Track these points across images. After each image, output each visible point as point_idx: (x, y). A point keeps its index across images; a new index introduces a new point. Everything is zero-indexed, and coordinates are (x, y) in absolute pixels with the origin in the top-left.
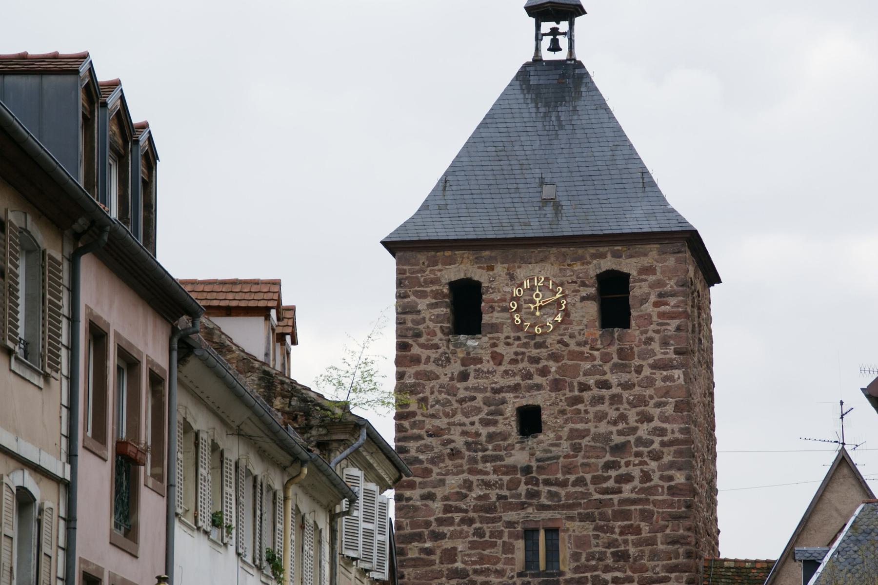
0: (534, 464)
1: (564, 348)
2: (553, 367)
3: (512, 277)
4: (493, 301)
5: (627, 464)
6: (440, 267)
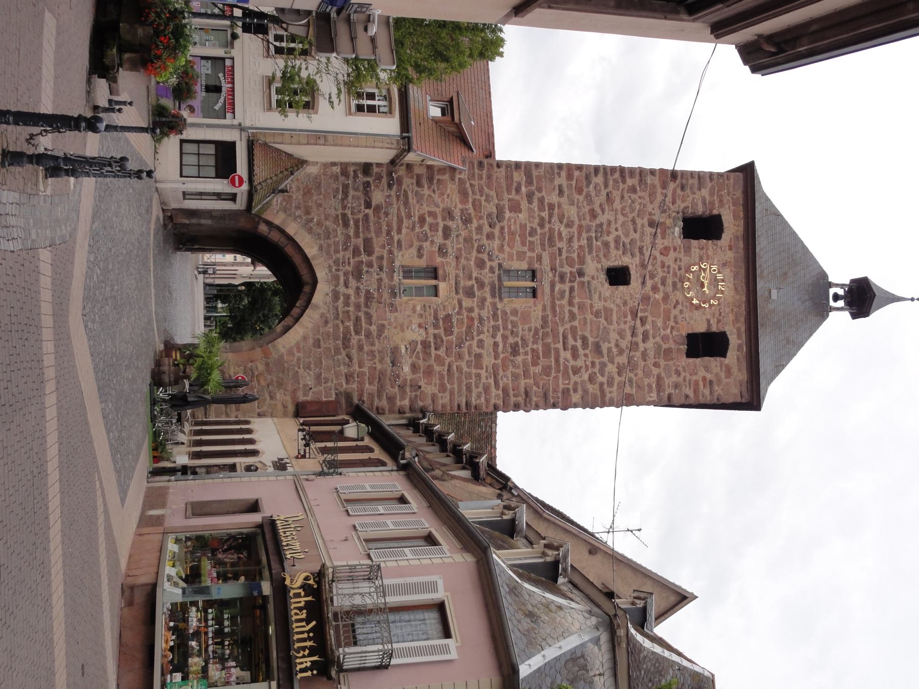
0: (586, 279)
1: (673, 305)
2: (659, 296)
3: (724, 265)
4: (707, 249)
5: (586, 355)
6: (732, 208)
